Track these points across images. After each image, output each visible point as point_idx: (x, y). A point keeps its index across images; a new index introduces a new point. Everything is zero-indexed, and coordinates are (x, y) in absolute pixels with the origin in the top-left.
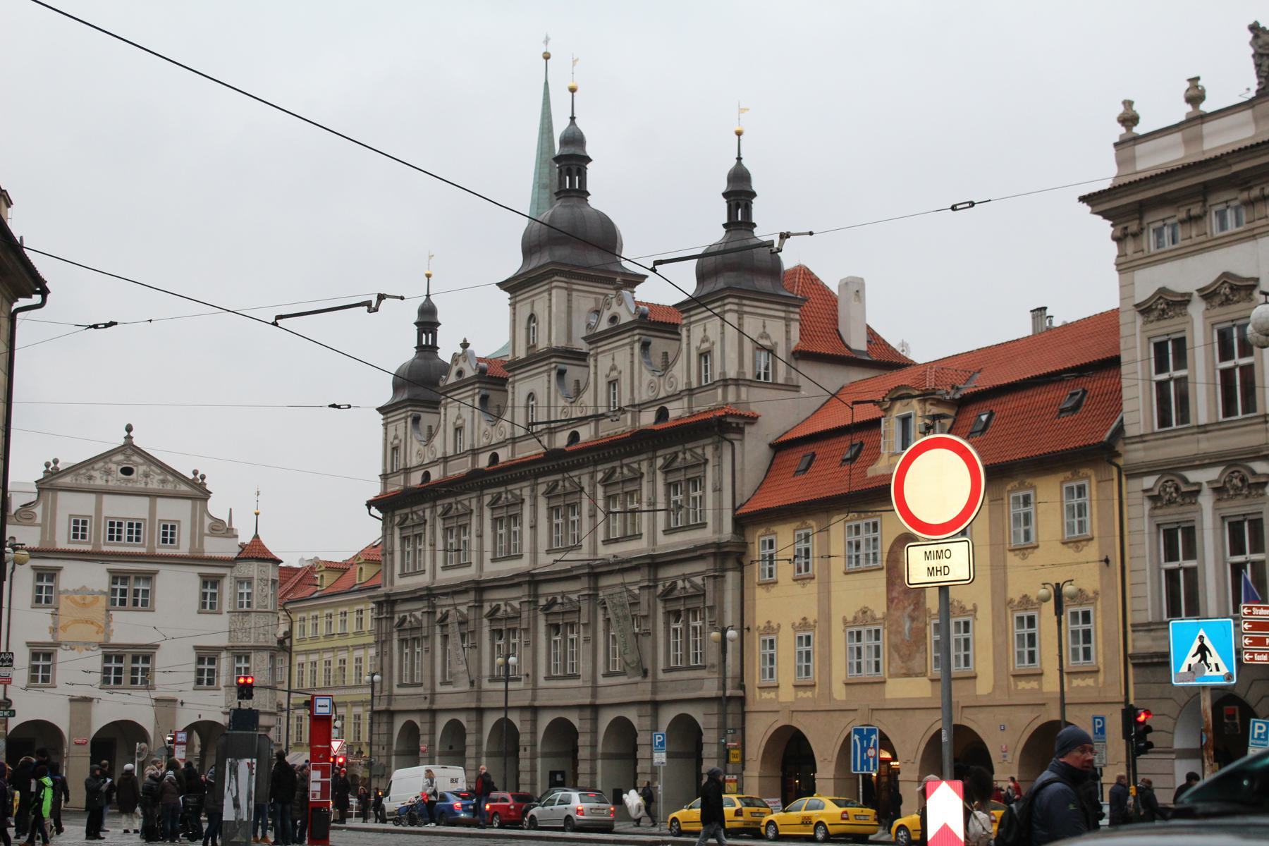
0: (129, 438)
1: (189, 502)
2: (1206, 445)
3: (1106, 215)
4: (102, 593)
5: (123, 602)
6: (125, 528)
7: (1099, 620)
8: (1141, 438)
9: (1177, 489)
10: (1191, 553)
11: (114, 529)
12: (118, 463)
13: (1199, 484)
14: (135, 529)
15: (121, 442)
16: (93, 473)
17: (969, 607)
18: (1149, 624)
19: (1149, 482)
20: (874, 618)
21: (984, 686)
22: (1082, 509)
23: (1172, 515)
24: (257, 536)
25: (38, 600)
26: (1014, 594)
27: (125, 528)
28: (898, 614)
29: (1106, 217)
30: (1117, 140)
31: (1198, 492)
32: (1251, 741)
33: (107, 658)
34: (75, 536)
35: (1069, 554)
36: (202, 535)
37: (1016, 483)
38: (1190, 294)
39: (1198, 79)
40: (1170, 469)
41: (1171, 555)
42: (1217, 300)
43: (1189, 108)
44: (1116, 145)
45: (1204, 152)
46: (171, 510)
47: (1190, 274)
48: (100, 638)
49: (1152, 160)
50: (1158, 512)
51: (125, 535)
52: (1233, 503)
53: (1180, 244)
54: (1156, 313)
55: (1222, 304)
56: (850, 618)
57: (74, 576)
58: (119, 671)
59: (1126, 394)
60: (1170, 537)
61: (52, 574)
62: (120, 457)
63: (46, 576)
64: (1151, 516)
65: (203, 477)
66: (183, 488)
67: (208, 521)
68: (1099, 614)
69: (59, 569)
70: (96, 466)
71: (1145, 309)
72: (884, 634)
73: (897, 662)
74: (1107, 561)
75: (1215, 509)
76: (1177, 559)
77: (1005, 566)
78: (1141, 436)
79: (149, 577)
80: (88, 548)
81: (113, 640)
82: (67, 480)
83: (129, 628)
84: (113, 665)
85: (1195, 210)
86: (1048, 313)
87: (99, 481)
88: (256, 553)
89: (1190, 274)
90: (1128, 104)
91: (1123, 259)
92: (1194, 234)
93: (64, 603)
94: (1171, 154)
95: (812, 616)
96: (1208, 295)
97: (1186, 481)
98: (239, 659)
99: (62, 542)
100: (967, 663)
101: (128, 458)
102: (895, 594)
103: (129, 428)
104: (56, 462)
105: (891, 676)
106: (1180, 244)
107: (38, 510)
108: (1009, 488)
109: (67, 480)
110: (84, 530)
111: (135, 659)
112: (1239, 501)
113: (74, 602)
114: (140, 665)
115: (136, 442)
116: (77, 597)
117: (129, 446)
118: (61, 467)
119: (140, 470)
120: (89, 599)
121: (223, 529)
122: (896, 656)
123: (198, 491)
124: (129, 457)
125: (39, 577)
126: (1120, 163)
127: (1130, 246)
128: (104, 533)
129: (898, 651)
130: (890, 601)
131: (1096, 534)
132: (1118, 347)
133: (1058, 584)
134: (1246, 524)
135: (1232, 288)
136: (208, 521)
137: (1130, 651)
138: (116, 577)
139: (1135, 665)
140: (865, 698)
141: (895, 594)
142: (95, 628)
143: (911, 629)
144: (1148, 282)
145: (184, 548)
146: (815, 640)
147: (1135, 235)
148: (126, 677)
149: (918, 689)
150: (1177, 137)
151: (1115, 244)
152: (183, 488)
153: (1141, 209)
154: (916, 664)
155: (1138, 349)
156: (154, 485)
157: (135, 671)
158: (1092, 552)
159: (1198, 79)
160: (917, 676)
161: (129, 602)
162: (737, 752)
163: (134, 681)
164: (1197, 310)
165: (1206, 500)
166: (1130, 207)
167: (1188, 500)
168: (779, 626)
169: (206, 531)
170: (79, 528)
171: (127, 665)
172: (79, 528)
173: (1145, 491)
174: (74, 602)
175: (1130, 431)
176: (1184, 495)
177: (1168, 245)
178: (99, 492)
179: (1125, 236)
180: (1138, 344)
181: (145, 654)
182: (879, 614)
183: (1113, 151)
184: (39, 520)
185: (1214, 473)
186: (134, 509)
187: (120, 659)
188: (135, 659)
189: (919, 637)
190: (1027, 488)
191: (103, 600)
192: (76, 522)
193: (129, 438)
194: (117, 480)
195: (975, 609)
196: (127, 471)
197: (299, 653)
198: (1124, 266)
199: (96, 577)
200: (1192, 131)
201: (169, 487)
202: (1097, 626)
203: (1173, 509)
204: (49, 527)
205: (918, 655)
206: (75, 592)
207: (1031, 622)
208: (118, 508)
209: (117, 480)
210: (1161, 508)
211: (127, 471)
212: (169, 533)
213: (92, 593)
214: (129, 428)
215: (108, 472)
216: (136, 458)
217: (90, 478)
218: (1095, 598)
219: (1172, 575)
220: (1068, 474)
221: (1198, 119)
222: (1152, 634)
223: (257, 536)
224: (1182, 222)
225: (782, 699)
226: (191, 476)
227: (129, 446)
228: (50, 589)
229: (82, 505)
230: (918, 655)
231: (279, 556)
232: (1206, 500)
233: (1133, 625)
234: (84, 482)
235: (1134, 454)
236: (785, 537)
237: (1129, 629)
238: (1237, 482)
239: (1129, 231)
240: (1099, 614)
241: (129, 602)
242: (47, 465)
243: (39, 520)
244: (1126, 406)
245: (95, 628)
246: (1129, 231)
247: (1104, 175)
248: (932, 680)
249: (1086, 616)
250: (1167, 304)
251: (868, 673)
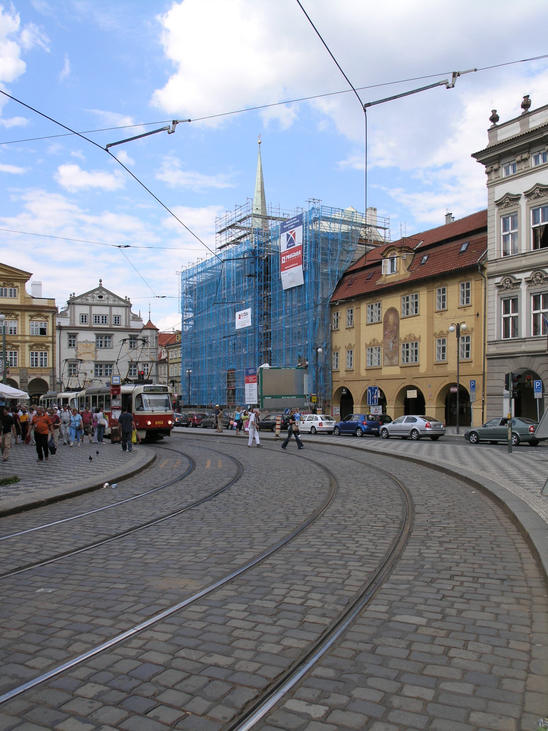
0: (101, 284)
1: (124, 308)
2: (524, 262)
3: (482, 162)
4: (93, 342)
5: (101, 346)
6: (101, 318)
7: (473, 340)
8: (495, 261)
9: (511, 282)
10: (515, 310)
11: (97, 318)
12: (97, 294)
13: (521, 279)
14: (105, 318)
15: (98, 286)
16: (88, 298)
17: (417, 337)
18: (495, 341)
19: (498, 280)
20: (378, 343)
21: (423, 369)
22: (468, 293)
23: (508, 293)
24: (150, 321)
25: (70, 345)
26: (437, 331)
27: (101, 318)
28: (388, 340)
29: (483, 164)
30: (489, 128)
31: (520, 283)
32: (535, 390)
33: (96, 366)
34: (82, 322)
35: (461, 312)
36: (130, 320)
37: (439, 284)
38: (521, 195)
39: (528, 96)
40: (508, 274)
41: (507, 311)
42: (533, 197)
43: (523, 110)
44: (489, 130)
45: (529, 129)
46: (116, 311)
47: (521, 186)
48: (94, 359)
49: (504, 135)
50: (502, 293)
51: (101, 321)
52: (536, 287)
53: (517, 172)
54: (504, 205)
55: (535, 198)
56: (368, 343)
57: (82, 336)
58: (101, 371)
59: (489, 242)
60: (506, 303)
61: (74, 336)
62: (98, 292)
63: (73, 336)
64: (498, 295)
65: (129, 299)
66: (122, 303)
67: (131, 315)
68: (473, 337)
69: (77, 334)
70: (89, 295)
71: (499, 204)
72: (382, 349)
73: (387, 361)
74: (478, 315)
75: (528, 290)
76: (509, 313)
77: (433, 318)
78: (496, 260)
79: (110, 336)
80: (88, 326)
81: (98, 359)
82: (78, 301)
83: (104, 355)
84: (99, 368)
85: (525, 156)
86: (453, 216)
87: (90, 301)
88: (150, 327)
89: (521, 186)
90: (494, 112)
91: (490, 182)
92: (523, 168)
93: (80, 347)
94: (515, 131)
95: (353, 343)
96: (528, 195)
97: (515, 279)
98: (145, 365)
99: (78, 324)
100: (416, 360)
101: (101, 292)
102: (387, 333)
103: (101, 281)
104: (74, 294)
105: (384, 366)
106: (517, 172)
107: (68, 312)
108: (436, 286)
109: (78, 301)
110: (85, 319)
111: (107, 366)
112: (539, 286)
113: (83, 345)
114: (109, 368)
115: (104, 286)
116: (84, 344)
117: (101, 288)
118: (76, 296)
119: (105, 297)
120: (89, 344)
121: (137, 318)
122: (386, 358)
123: (127, 305)
124: (100, 292)
125: (70, 337)
126: (490, 138)
127: (493, 176)
128: (93, 320)
129: (387, 356)
130: (385, 335)
131: (473, 304)
132: (486, 222)
133: (458, 324)
134: (541, 296)
135: (540, 191)
136: (131, 315)
137: (486, 353)
138: (98, 336)
139: (488, 359)
140: (373, 374)
141: (387, 333)
142: (91, 355)
143: (393, 347)
144: (500, 192)
145: (123, 325)
146: (354, 353)
147: (496, 170)
148: (103, 373)
149: (395, 371)
150: (518, 123)
151: (487, 175)
152: (122, 303)
153: (499, 158)
154: (395, 361)
155: (496, 221)
156: (111, 302)
157: (107, 370)
158: (471, 311)
159: (528, 96)
160: (395, 365)
161: (103, 346)
162: (315, 397)
163: (107, 374)
164: (523, 202)
165: (524, 287)
166: (493, 157)
167: (515, 287)
168: (340, 347)
169: (131, 319)
170: (84, 318)
171: (103, 368)
172: (84, 318)
173: (496, 284)
174: (83, 345)
175: (490, 258)
176: (514, 284)
177: (511, 173)
178: (91, 305)
179: (492, 171)
180: (496, 219)
181: (110, 364)
182: (380, 341)
183: (487, 133)
184: (69, 316)
185: (528, 274)
186: (105, 311)
187: (101, 366)
188: (107, 366)
189: (396, 351)
190: (444, 285)
191: (94, 345)
192: (82, 316)
193: (101, 284)
194: (97, 300)
195: (420, 338)
196: (101, 297)
197: (170, 364)
198: (490, 185)
199: (91, 337)
200: (524, 120)
201: (116, 303)
202: (472, 342)
203: (508, 291)
204: (73, 319)
205: (396, 357)
206: (84, 342)
207: (444, 341)
208: (97, 310)
209: (97, 300)
210: (502, 291)
211: (101, 297)
212: (117, 319)
213: (90, 342)
214: (101, 281)
215: (94, 298)
216: (103, 292)
217: (87, 300)
218: (472, 331)
219: (506, 320)
220: (462, 278)
221: (526, 115)
222: (497, 345)
223: (150, 321)
224: (519, 162)
225: (340, 376)
226: (124, 299)
227: (101, 288)
228: (74, 341)
229: (85, 310)
230: (396, 357)
231: (157, 327)
232: (524, 287)
233: (488, 342)
234: (84, 301)
235: (491, 268)
236: (343, 313)
237: (486, 344)
238: (538, 277)
239: (494, 168)
240: (473, 337)
241: (103, 346)
242: (71, 295)
243: (69, 316)
244: (489, 247)
245: (91, 355)
246: (494, 168)
247: (483, 144)
248: (401, 367)
249: (468, 338)
250: (510, 200)
251: (375, 364)
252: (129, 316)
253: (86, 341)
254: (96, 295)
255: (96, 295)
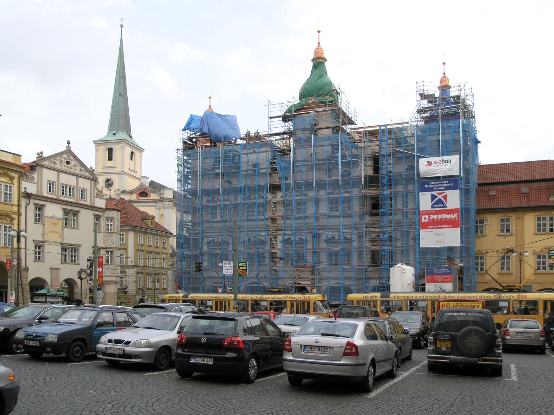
0: (68, 147)
4: (60, 219)
12: (65, 158)
15: (64, 149)
48: (60, 240)
62: (65, 156)
63: (39, 208)
66: (88, 174)
69: (44, 206)
80: (55, 197)
83: (71, 237)
87: (58, 166)
93: (46, 222)
99: (45, 193)
103: (69, 143)
113: (50, 222)
115: (72, 149)
116: (51, 220)
118: (45, 155)
119: (73, 163)
120: (56, 221)
152: (88, 174)
156: (78, 172)
174: (50, 222)
178: (59, 171)
191: (61, 223)
201: (83, 173)
206: (51, 217)
209: (64, 167)
211: (68, 163)
213: (56, 218)
214: (69, 143)
217: (55, 163)
227: (69, 151)
234: (52, 165)
243: (36, 181)
252: (94, 191)
253: (53, 217)
254: (63, 159)
255: (63, 159)
